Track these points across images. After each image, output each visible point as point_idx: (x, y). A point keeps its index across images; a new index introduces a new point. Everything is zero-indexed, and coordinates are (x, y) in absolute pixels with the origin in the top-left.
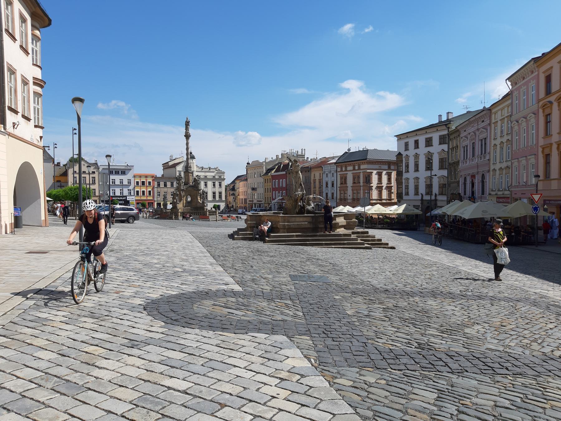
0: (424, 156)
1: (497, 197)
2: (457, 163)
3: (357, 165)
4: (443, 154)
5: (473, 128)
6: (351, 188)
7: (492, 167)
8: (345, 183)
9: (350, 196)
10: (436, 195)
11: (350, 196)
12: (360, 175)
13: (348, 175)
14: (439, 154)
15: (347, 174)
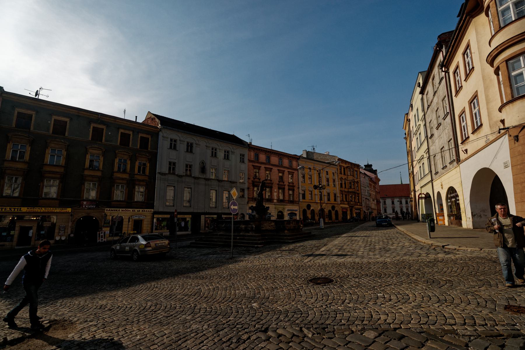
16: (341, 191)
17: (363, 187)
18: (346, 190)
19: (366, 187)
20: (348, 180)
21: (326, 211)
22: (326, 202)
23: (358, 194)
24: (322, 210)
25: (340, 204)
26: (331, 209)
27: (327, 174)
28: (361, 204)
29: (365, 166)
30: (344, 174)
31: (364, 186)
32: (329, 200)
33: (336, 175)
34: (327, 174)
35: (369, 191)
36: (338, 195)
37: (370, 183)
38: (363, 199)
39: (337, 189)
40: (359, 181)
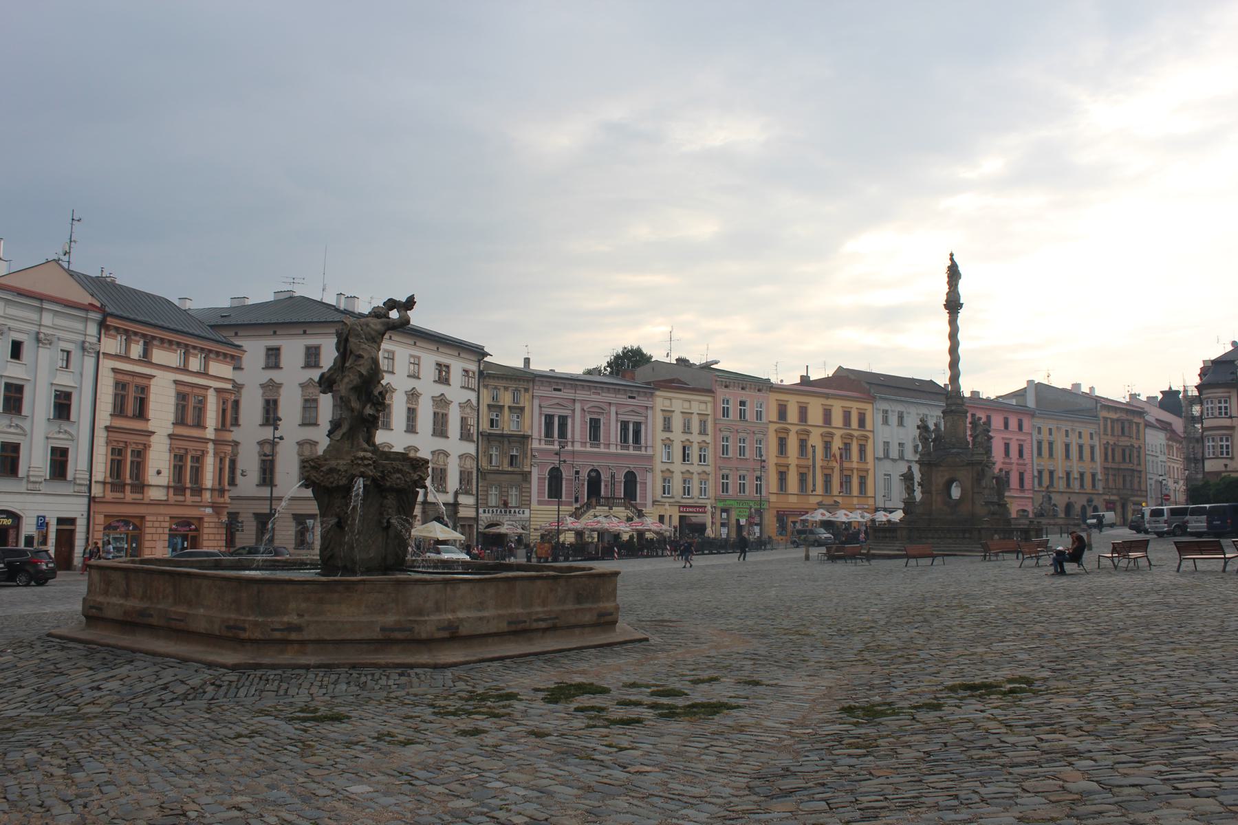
0: (431, 403)
1: (680, 506)
2: (524, 439)
3: (195, 356)
4: (468, 410)
5: (600, 397)
6: (168, 441)
7: (659, 467)
8: (141, 414)
9: (159, 473)
10: (456, 494)
11: (159, 473)
12: (205, 397)
13: (153, 382)
14: (461, 407)
15: (151, 377)
16: (1104, 468)
17: (1153, 456)
18: (1114, 466)
19: (1158, 454)
20: (1118, 446)
21: (1078, 508)
22: (1077, 491)
23: (1140, 472)
24: (1069, 507)
25: (1104, 494)
26: (1085, 504)
27: (1080, 437)
28: (1144, 493)
29: (1162, 392)
30: (1113, 435)
31: (1154, 454)
32: (1082, 486)
33: (1096, 438)
34: (1080, 437)
35: (1164, 462)
36: (1099, 477)
37: (1170, 443)
38: (1149, 482)
39: (1098, 466)
40: (1142, 446)
